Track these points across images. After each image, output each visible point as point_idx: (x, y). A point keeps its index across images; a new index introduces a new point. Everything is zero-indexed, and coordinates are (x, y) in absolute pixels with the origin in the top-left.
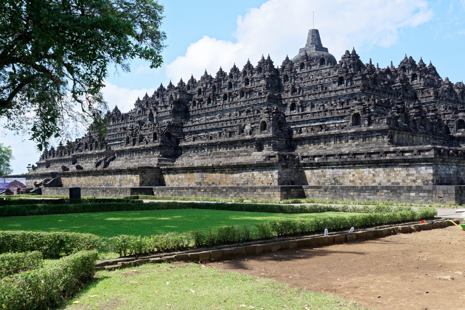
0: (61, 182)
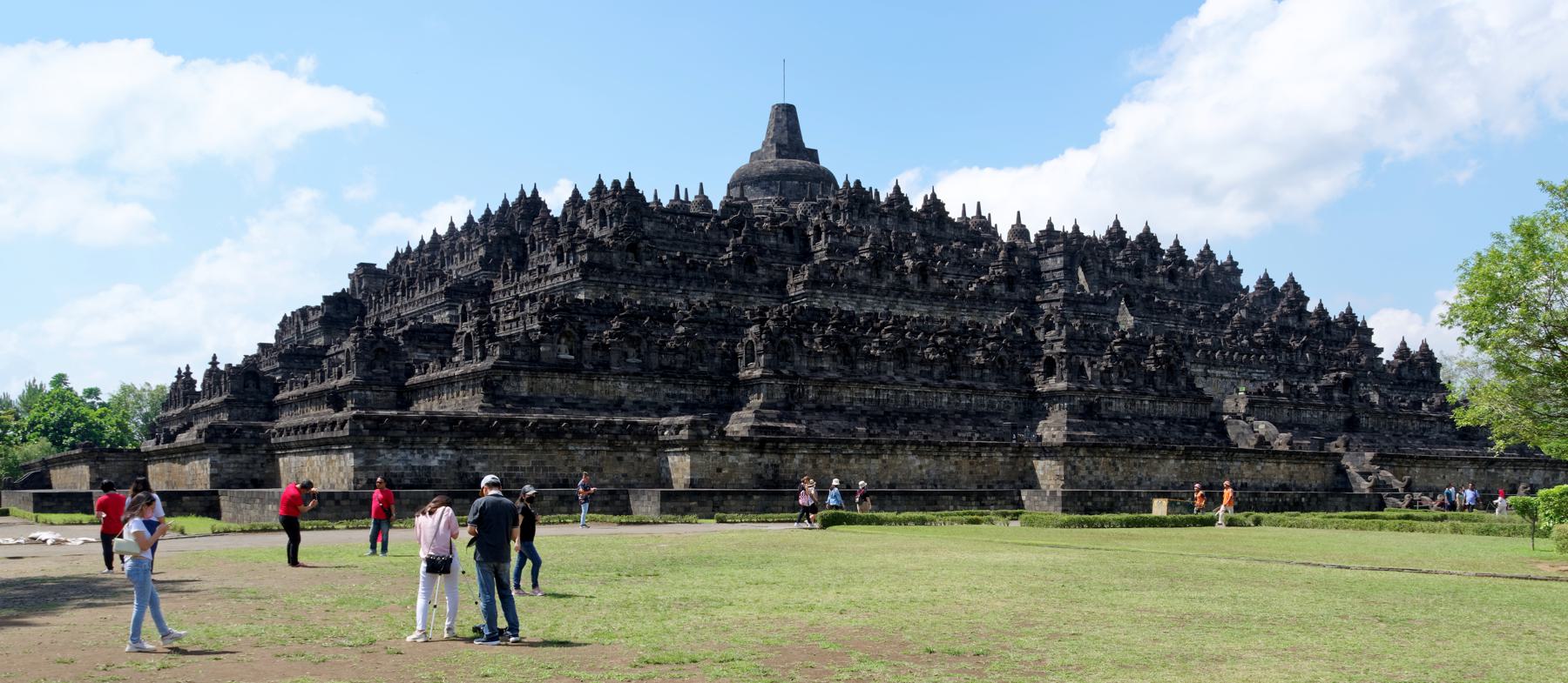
0: (49, 480)
